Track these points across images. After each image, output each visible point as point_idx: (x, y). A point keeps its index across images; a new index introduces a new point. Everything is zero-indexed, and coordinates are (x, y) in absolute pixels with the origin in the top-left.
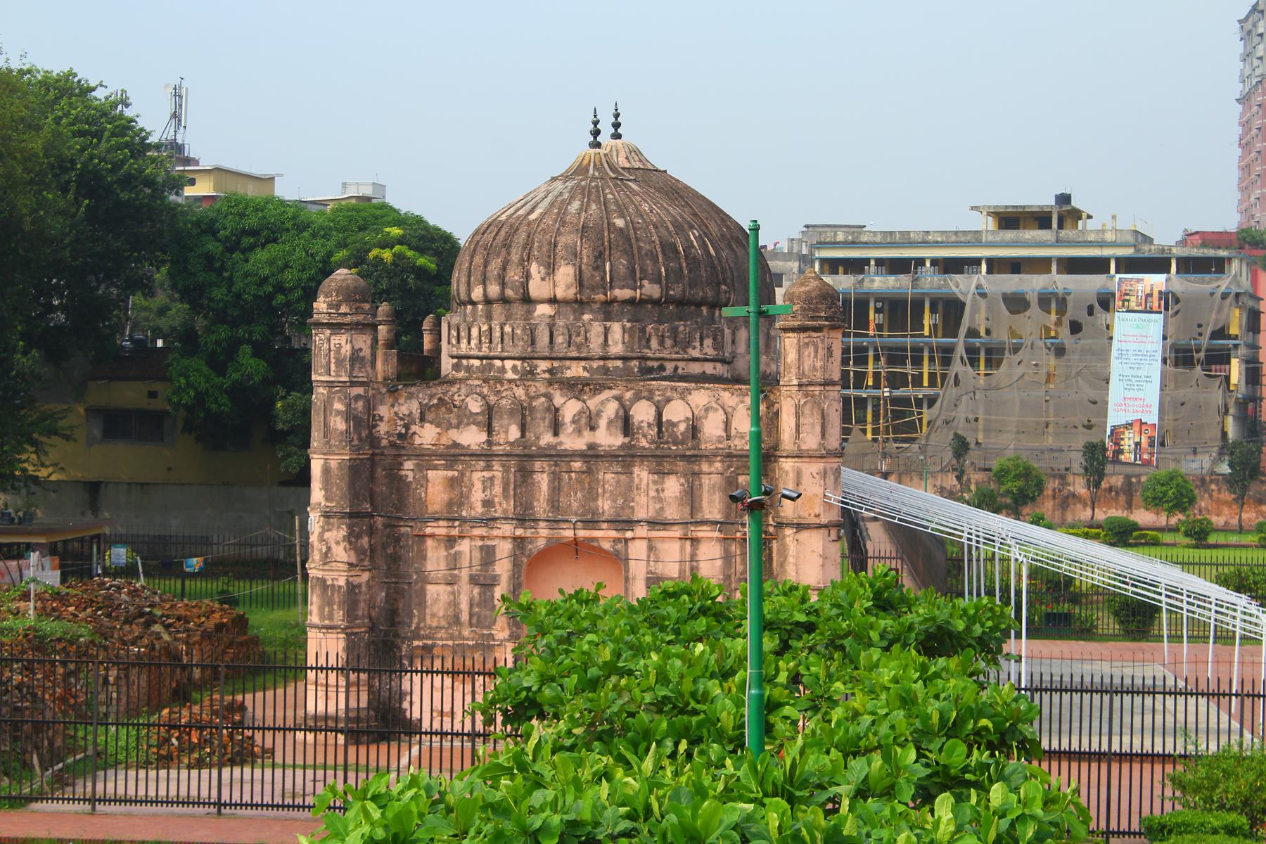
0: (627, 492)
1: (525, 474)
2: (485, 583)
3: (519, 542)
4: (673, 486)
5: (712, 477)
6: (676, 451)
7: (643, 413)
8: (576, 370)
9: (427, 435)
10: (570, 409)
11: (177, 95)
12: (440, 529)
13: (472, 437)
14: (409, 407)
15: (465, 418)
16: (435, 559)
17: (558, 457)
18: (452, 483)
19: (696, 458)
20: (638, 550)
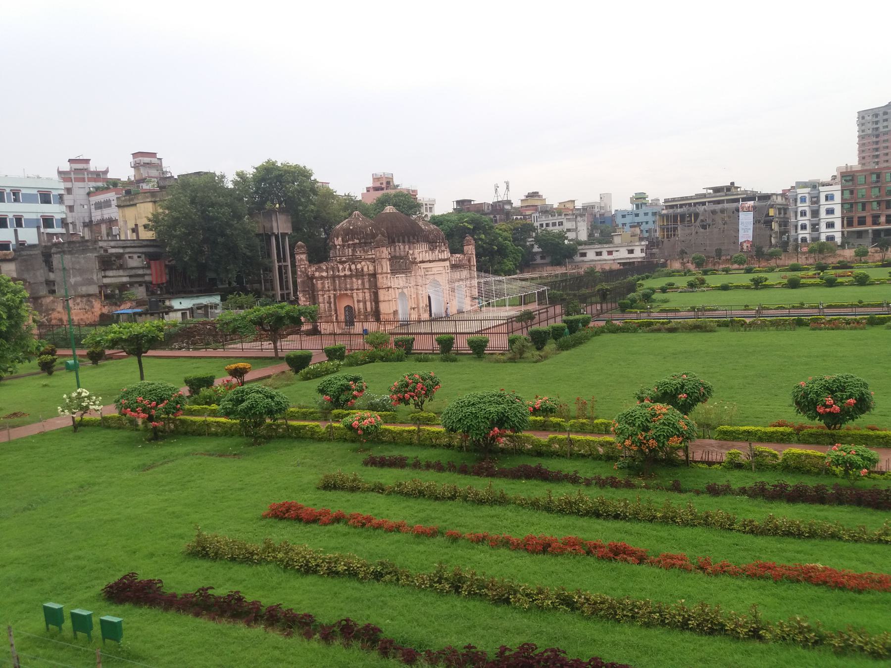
0: (352, 283)
1: (334, 281)
2: (330, 303)
3: (335, 295)
4: (360, 282)
5: (366, 278)
6: (359, 274)
7: (353, 267)
8: (344, 259)
9: (317, 274)
10: (341, 267)
11: (507, 184)
12: (320, 293)
13: (324, 274)
14: (314, 269)
15: (323, 271)
16: (321, 300)
17: (339, 277)
18: (322, 283)
19: (363, 275)
20: (355, 295)
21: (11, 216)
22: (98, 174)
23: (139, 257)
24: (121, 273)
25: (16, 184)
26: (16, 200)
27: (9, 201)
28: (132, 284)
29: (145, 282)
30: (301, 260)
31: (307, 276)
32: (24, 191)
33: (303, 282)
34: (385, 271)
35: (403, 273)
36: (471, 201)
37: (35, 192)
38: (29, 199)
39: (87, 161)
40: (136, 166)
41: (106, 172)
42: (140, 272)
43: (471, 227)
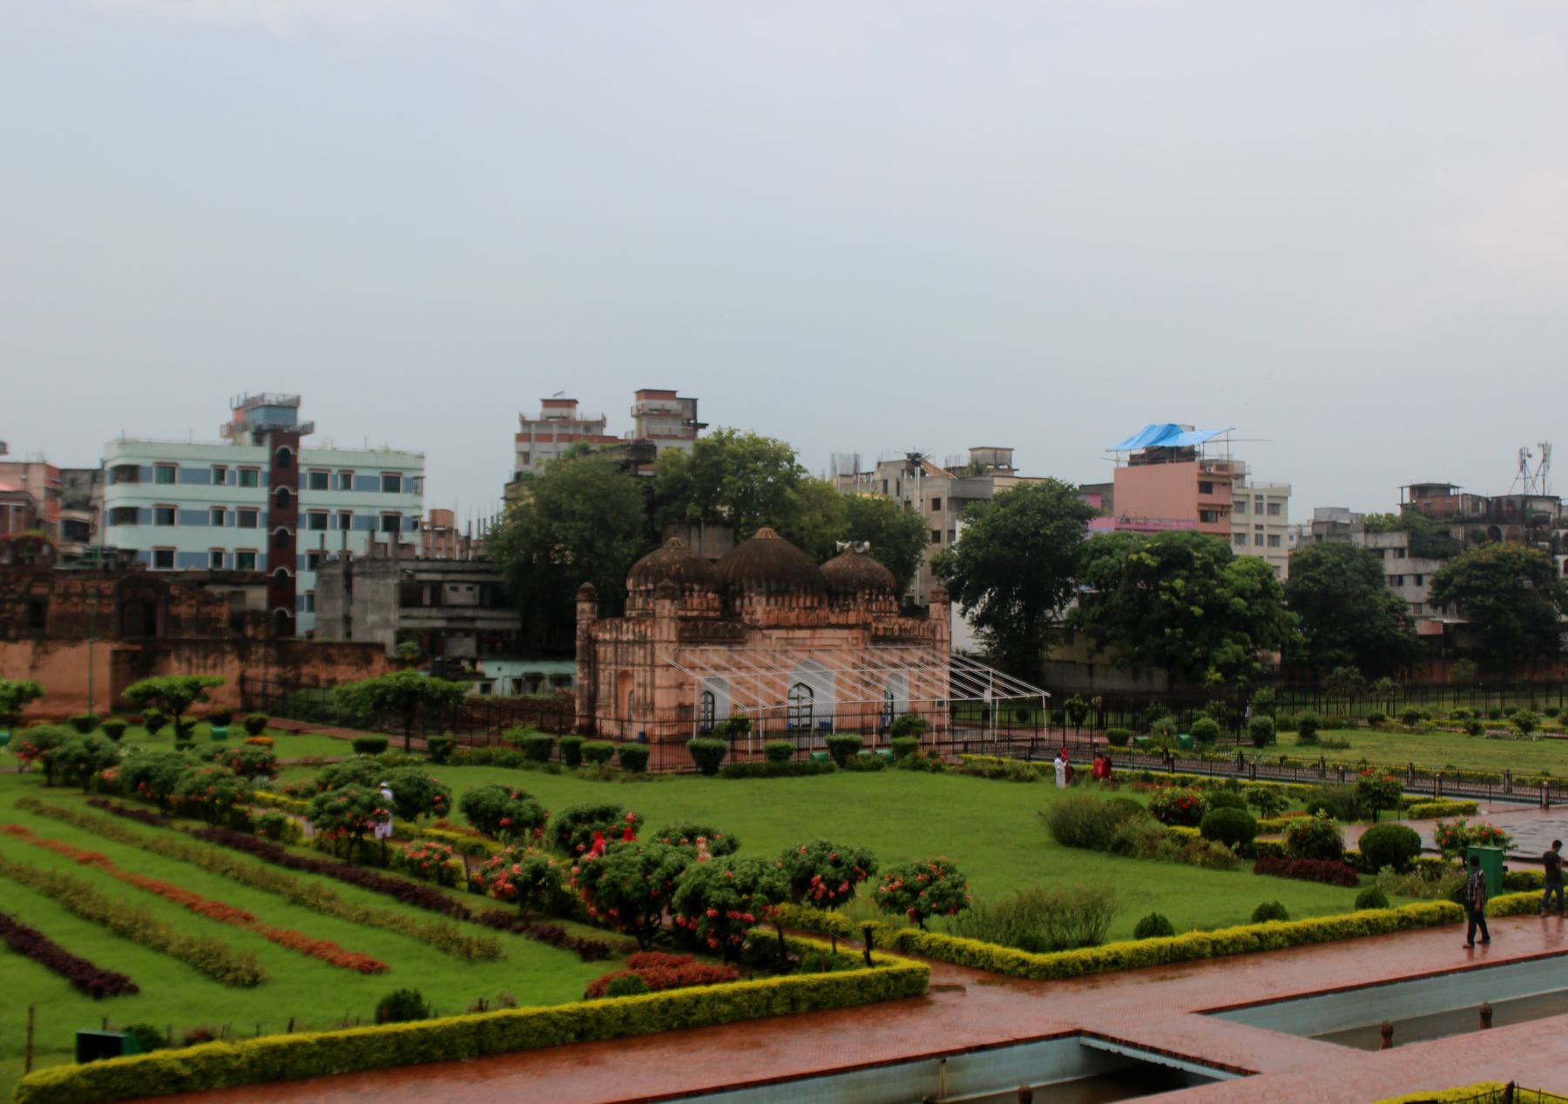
11: (1546, 449)
13: (607, 637)
17: (621, 642)
21: (334, 511)
22: (588, 425)
23: (470, 589)
24: (434, 612)
25: (348, 462)
26: (347, 486)
27: (335, 488)
28: (451, 632)
29: (475, 630)
30: (583, 611)
31: (589, 637)
32: (359, 473)
33: (582, 647)
34: (665, 637)
35: (721, 643)
36: (1446, 488)
37: (376, 473)
38: (367, 484)
39: (572, 403)
40: (640, 415)
41: (601, 424)
42: (469, 613)
43: (1151, 561)
